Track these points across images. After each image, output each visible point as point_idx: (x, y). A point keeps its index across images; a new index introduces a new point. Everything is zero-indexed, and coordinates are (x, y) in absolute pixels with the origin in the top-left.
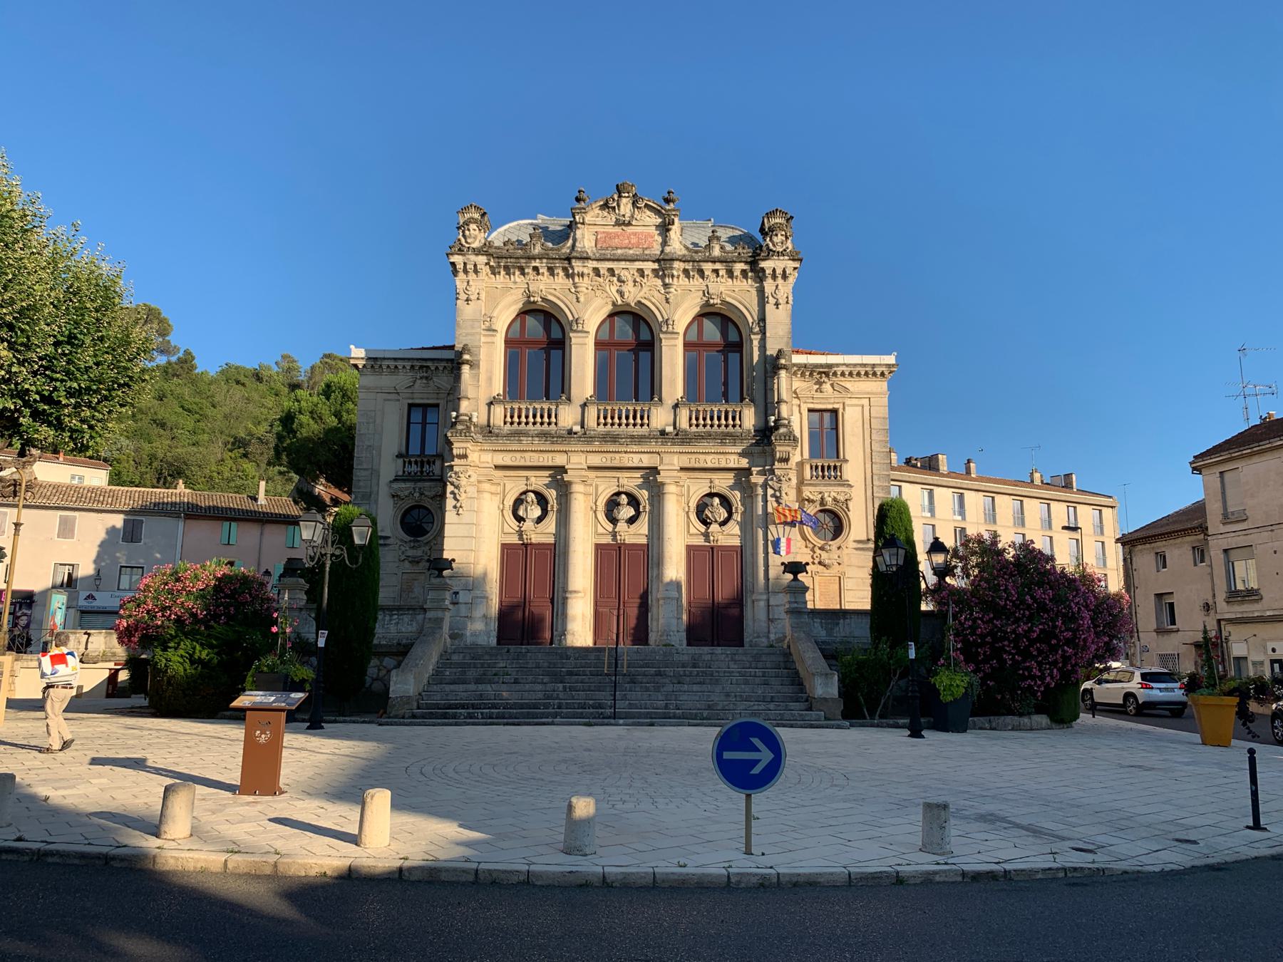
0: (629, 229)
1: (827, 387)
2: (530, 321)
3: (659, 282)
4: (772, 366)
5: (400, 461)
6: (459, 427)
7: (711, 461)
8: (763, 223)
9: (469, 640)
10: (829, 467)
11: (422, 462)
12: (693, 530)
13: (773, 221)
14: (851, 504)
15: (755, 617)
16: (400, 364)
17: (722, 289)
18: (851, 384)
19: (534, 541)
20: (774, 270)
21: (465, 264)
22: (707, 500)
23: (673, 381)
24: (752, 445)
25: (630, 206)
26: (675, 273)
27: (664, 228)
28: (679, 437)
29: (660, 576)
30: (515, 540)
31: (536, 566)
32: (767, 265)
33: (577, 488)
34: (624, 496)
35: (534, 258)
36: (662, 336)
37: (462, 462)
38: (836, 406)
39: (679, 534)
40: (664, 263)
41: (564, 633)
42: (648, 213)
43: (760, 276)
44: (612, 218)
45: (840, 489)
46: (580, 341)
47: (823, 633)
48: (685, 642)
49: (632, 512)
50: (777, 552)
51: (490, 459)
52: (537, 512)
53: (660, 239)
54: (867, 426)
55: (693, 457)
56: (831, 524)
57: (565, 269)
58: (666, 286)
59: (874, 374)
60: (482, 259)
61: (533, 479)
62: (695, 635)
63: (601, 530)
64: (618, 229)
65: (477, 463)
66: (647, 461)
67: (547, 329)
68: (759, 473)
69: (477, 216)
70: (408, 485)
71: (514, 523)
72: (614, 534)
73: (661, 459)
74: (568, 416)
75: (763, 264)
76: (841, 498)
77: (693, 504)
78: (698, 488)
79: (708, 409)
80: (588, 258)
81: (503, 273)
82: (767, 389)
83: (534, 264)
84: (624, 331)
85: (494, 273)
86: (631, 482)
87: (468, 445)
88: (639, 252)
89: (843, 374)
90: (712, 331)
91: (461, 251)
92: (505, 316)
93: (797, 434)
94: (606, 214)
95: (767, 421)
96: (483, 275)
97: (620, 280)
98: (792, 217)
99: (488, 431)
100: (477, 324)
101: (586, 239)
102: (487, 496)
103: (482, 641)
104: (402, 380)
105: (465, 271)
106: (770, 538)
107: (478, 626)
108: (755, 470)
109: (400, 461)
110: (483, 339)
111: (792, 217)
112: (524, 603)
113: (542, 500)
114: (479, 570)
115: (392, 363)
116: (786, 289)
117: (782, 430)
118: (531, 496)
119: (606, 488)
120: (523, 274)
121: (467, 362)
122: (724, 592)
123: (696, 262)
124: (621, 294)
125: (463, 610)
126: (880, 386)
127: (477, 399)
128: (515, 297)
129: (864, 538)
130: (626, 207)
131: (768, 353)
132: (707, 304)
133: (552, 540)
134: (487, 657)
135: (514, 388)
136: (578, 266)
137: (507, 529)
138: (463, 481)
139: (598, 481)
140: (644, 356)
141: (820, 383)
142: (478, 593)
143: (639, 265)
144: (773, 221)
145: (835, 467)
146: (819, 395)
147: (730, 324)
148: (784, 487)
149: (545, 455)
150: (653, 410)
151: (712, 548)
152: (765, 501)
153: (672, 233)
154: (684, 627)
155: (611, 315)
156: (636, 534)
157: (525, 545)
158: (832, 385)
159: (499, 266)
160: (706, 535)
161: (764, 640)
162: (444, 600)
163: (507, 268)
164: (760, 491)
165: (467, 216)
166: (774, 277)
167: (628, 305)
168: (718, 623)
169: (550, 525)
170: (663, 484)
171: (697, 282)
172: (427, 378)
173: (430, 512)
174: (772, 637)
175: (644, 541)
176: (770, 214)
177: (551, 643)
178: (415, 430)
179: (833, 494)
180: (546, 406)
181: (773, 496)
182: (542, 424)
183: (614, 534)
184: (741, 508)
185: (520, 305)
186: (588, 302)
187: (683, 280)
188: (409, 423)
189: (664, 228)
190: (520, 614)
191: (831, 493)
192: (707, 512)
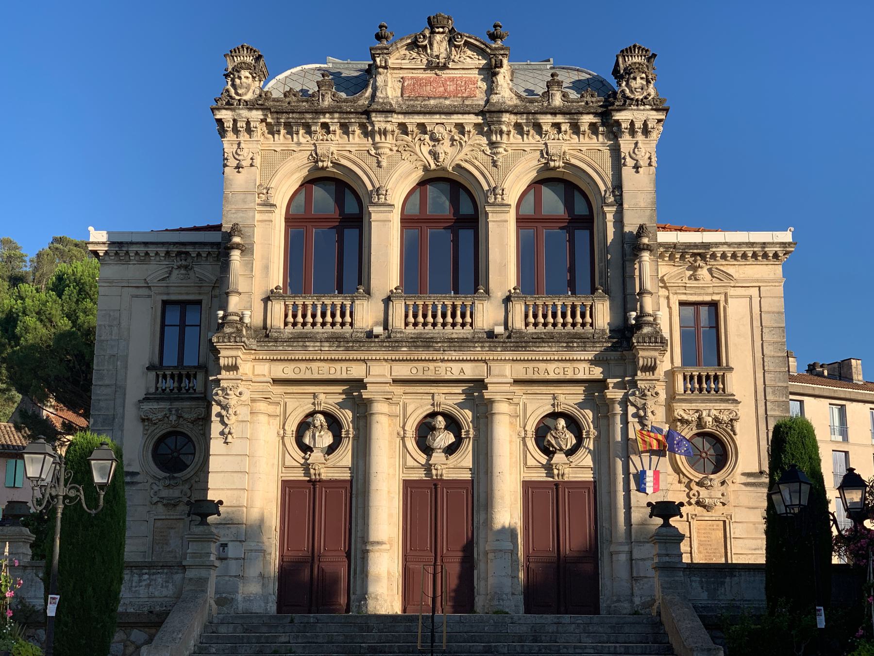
0: (445, 74)
1: (703, 273)
2: (318, 192)
3: (484, 140)
4: (632, 246)
5: (152, 375)
6: (228, 330)
7: (553, 371)
8: (617, 64)
9: (241, 606)
10: (708, 377)
11: (180, 376)
12: (531, 462)
13: (630, 60)
14: (737, 426)
15: (614, 575)
16: (152, 250)
17: (565, 148)
18: (737, 270)
19: (324, 477)
20: (632, 123)
21: (235, 121)
22: (549, 422)
23: (504, 266)
24: (607, 349)
25: (445, 44)
26: (504, 128)
27: (490, 72)
28: (512, 341)
29: (488, 520)
30: (299, 475)
31: (327, 509)
32: (623, 117)
33: (380, 407)
34: (440, 418)
35: (324, 113)
36: (488, 209)
37: (232, 375)
38: (716, 298)
39: (513, 467)
40: (489, 117)
41: (364, 596)
42: (469, 53)
43: (613, 131)
45: (723, 406)
46: (382, 216)
47: (705, 595)
48: (522, 608)
49: (451, 438)
50: (641, 489)
51: (266, 370)
52: (326, 439)
53: (484, 86)
54: (756, 323)
55: (531, 365)
56: (712, 452)
57: (363, 126)
58: (492, 144)
59: (765, 256)
60: (256, 115)
61: (322, 397)
62: (536, 597)
63: (410, 462)
64: (430, 74)
65: (251, 376)
66: (470, 371)
67: (340, 201)
68: (617, 386)
69: (249, 60)
71: (298, 454)
72: (428, 468)
73: (489, 370)
74: (367, 315)
76: (725, 417)
77: (531, 427)
78: (538, 406)
79: (550, 303)
80: (392, 112)
81: (283, 131)
83: (322, 120)
84: (440, 203)
85: (272, 133)
86: (449, 399)
87: (239, 353)
88: (457, 102)
89: (724, 256)
90: (552, 203)
91: (229, 106)
92: (286, 184)
93: (666, 334)
94: (415, 55)
95: (626, 319)
96: (257, 135)
97: (433, 138)
98: (654, 56)
99: (265, 334)
100: (249, 198)
101: (389, 87)
102: (263, 419)
103: (257, 607)
104: (154, 270)
105: (236, 131)
106: (632, 470)
107: (253, 588)
108: (611, 381)
109: (152, 375)
110: (258, 216)
111: (654, 56)
112: (312, 558)
113: (334, 424)
114: (254, 514)
115: (142, 249)
116: (647, 148)
117: (646, 330)
119: (417, 407)
120: (309, 132)
121: (237, 246)
122: (573, 541)
123: (531, 113)
124: (435, 155)
125: (233, 568)
126: (772, 272)
127: (250, 293)
128: (298, 163)
129: (756, 469)
130: (440, 46)
131: (627, 229)
132: (546, 168)
133: (347, 476)
134: (264, 629)
135: (297, 278)
136: (379, 122)
137: (289, 462)
138: (233, 400)
139: (407, 399)
140: (466, 235)
141: (694, 268)
142: (253, 545)
144: (630, 60)
145: (716, 377)
146: (694, 283)
147: (576, 193)
148: (650, 403)
149: (338, 366)
150: (478, 306)
151: (557, 484)
152: (625, 422)
153: (500, 78)
154: (520, 588)
155: (422, 184)
156: (458, 467)
157: (313, 482)
158: (710, 271)
159: (278, 124)
160: (549, 468)
161: (626, 605)
162: (208, 554)
163: (288, 126)
164: (618, 409)
165: (238, 60)
166: (632, 131)
167: (444, 169)
168: (566, 581)
169: (345, 456)
170: (491, 402)
171: (533, 139)
172: (186, 267)
173: (190, 439)
174: (637, 600)
175: (467, 476)
176: (626, 52)
177: (348, 610)
178: (172, 334)
179: (713, 412)
180: (338, 302)
181: (634, 416)
182: (333, 324)
183: (428, 468)
184: (593, 432)
185: (305, 172)
186: (392, 165)
187: (515, 138)
188: (163, 325)
189: (490, 72)
190: (307, 572)
191: (711, 411)
192: (549, 437)
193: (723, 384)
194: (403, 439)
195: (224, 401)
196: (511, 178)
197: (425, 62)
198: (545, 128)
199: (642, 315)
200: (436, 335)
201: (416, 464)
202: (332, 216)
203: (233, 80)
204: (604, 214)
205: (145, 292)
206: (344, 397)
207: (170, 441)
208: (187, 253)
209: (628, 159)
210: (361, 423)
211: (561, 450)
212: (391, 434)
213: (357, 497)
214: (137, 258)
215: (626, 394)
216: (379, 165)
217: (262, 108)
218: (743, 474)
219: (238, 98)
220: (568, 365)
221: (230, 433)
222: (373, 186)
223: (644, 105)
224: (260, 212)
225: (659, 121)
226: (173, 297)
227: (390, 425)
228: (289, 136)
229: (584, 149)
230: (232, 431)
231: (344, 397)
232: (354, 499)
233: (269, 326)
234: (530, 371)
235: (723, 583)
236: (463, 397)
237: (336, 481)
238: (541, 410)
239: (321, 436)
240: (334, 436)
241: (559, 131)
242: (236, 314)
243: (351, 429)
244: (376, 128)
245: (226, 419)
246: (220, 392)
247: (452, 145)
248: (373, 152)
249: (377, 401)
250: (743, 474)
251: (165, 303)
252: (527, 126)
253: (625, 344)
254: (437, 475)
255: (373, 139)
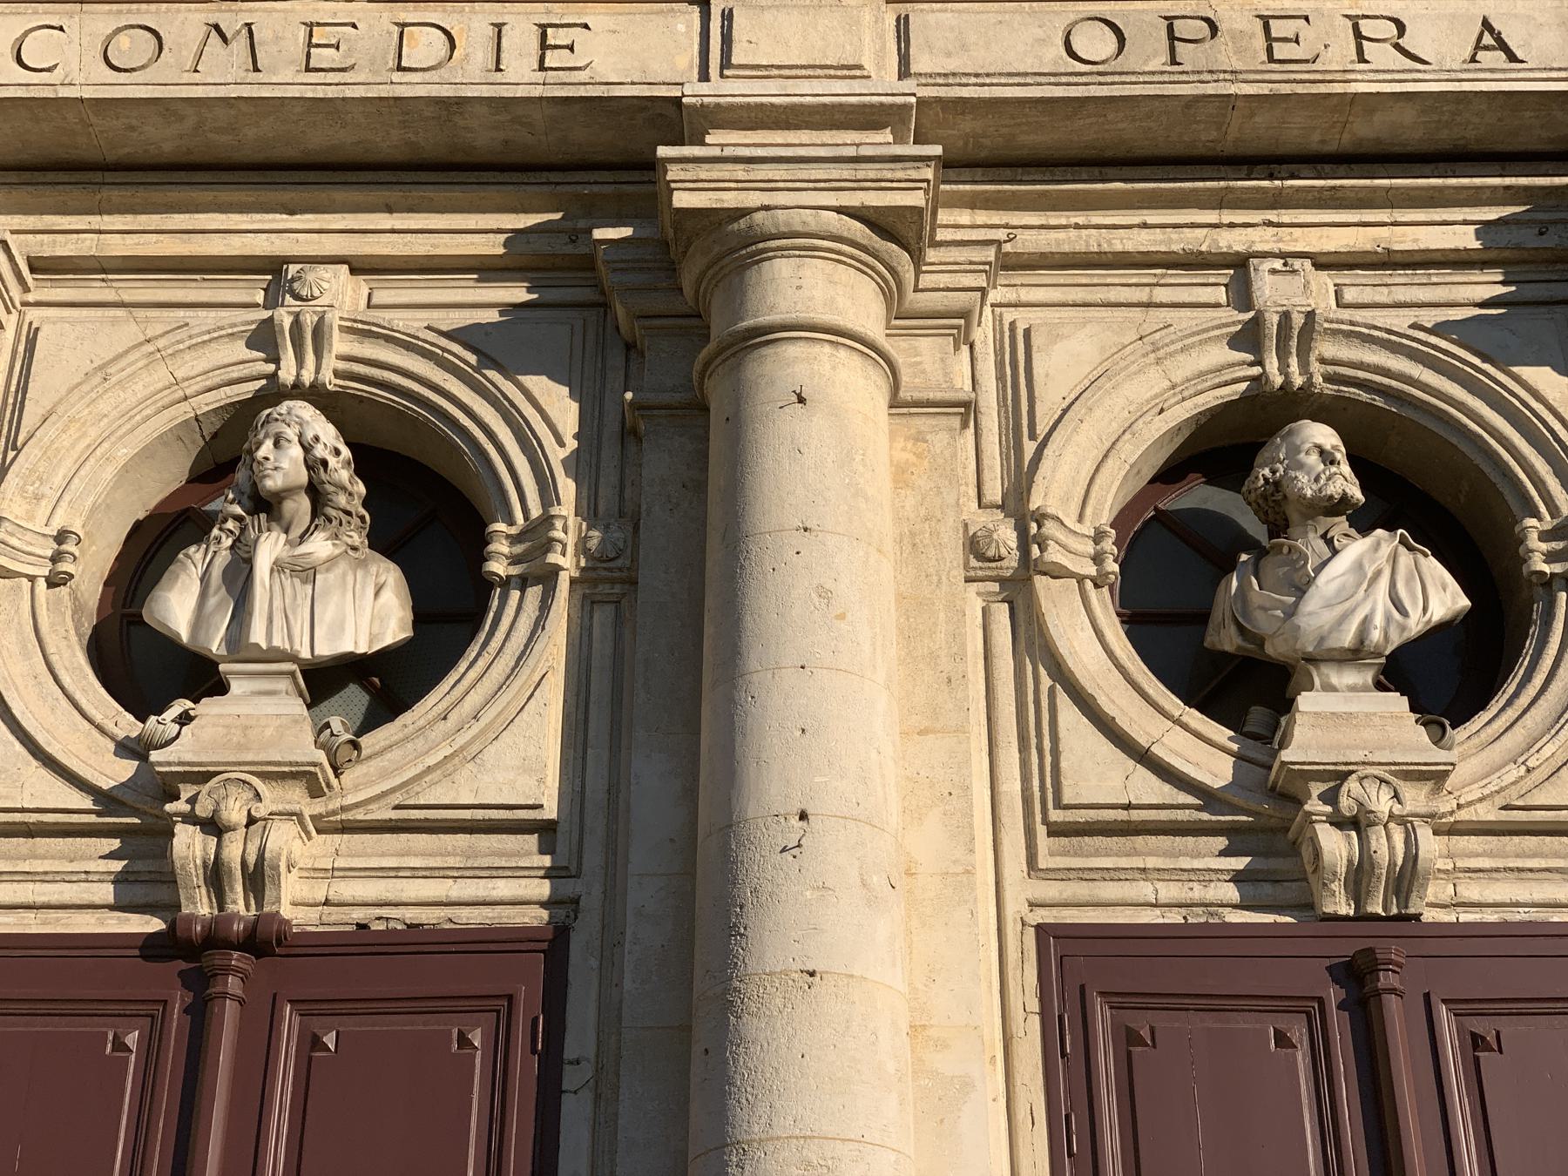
19: (296, 902)
63: (1096, 775)
71: (87, 730)
72: (1266, 822)
113: (423, 503)
157: (188, 953)
169: (507, 730)
194: (1017, 591)
201: (1148, 788)
206: (518, 293)
210: (659, 462)
212: (911, 543)
213: (604, 1091)
227: (901, 476)
231: (518, 293)
232: (575, 1113)
236: (1487, 285)
237: (417, 943)
239: (307, 573)
240: (422, 617)
249: (802, 242)
254: (1359, 876)
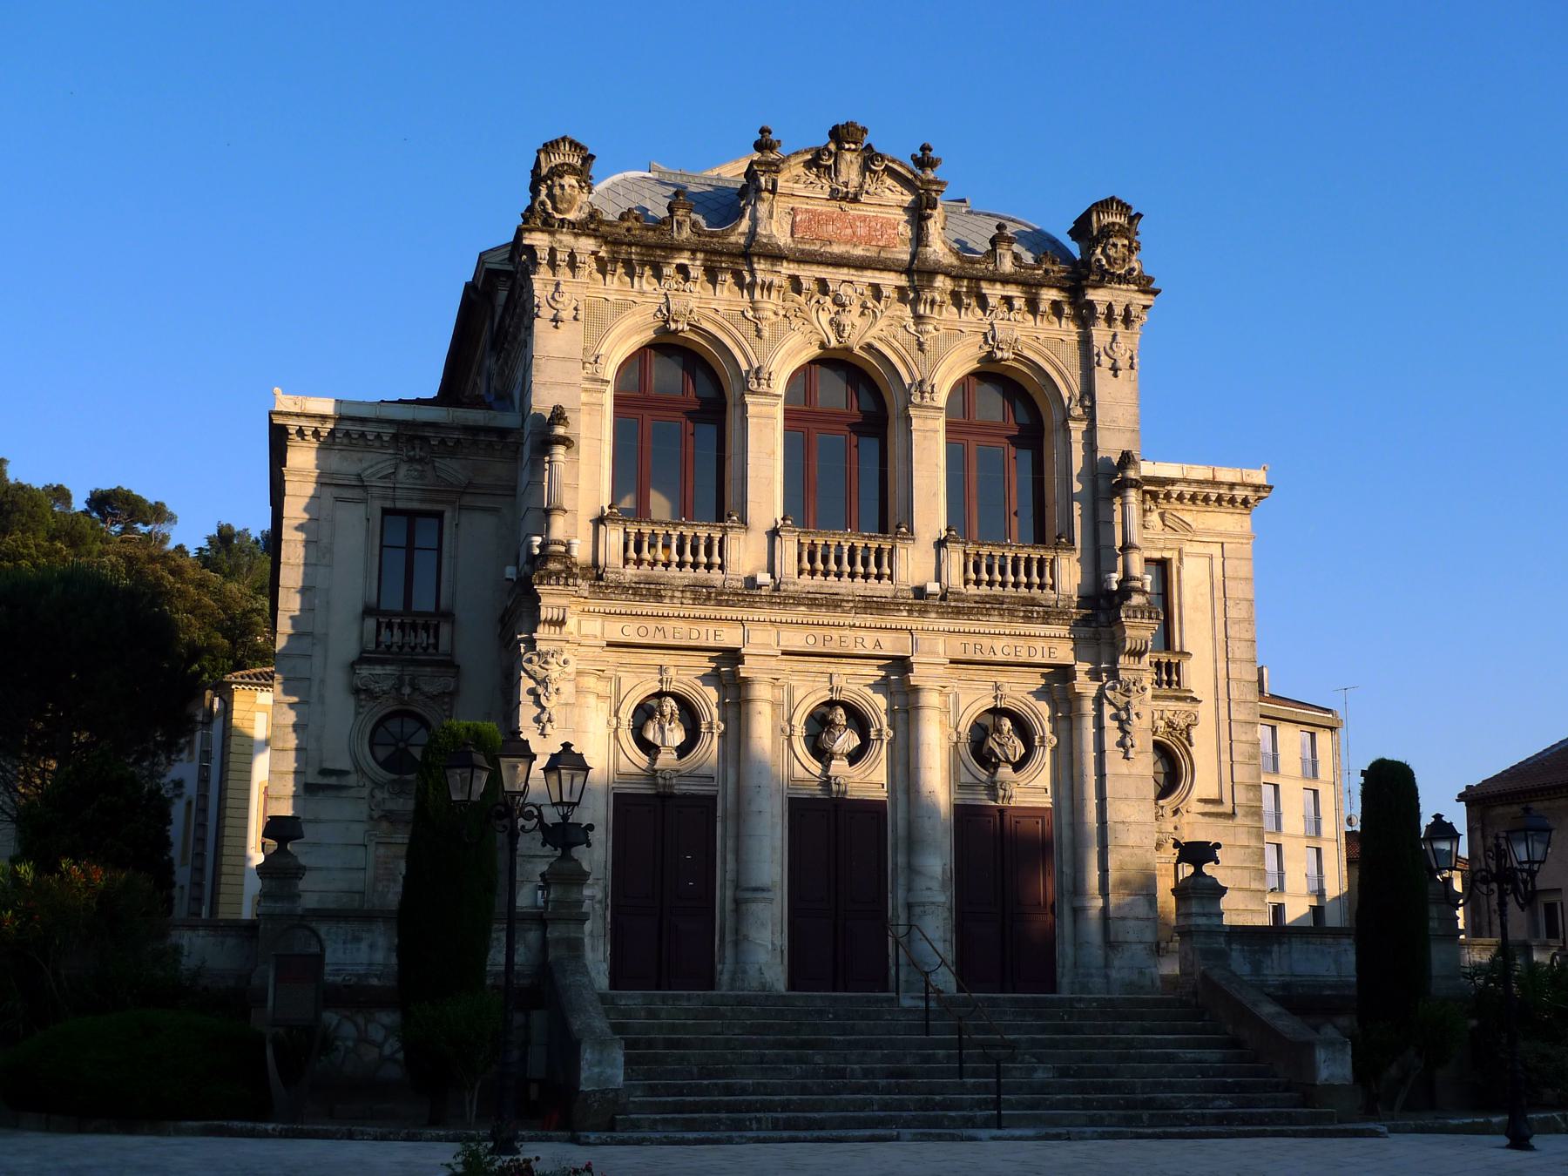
0: (853, 210)
5: (371, 623)
7: (1001, 649)
14: (1194, 732)
16: (369, 429)
18: (1193, 516)
21: (552, 251)
25: (856, 167)
28: (949, 604)
32: (1098, 296)
34: (841, 711)
36: (912, 412)
38: (1167, 555)
42: (889, 182)
44: (822, 188)
45: (1181, 705)
54: (1218, 594)
55: (972, 640)
57: (738, 277)
58: (919, 319)
60: (586, 245)
61: (672, 672)
66: (891, 645)
69: (576, 161)
70: (389, 669)
73: (915, 644)
75: (1093, 295)
76: (1181, 722)
78: (975, 699)
82: (1099, 525)
83: (678, 261)
88: (872, 253)
91: (548, 226)
94: (813, 178)
96: (583, 276)
101: (775, 223)
102: (592, 700)
105: (553, 264)
109: (371, 623)
111: (1139, 216)
118: (670, 705)
120: (658, 275)
123: (970, 281)
124: (838, 327)
127: (575, 513)
128: (638, 318)
129: (1214, 795)
130: (850, 169)
132: (989, 358)
138: (554, 671)
139: (795, 681)
143: (871, 277)
144: (1107, 219)
145: (1169, 664)
149: (703, 627)
150: (901, 551)
153: (930, 223)
158: (1162, 516)
159: (614, 261)
164: (1088, 707)
165: (556, 160)
166: (1110, 319)
167: (849, 350)
171: (973, 317)
179: (1168, 714)
180: (703, 533)
186: (777, 338)
189: (918, 214)
193: (1178, 675)
195: (541, 674)
196: (942, 369)
197: (826, 187)
198: (992, 301)
199: (1127, 577)
200: (842, 591)
202: (682, 399)
203: (550, 188)
204: (1068, 431)
205: (356, 493)
207: (410, 725)
208: (425, 440)
209: (1103, 357)
211: (1008, 761)
214: (345, 441)
215: (1102, 688)
216: (759, 336)
217: (594, 234)
218: (1200, 800)
219: (557, 216)
220: (1020, 642)
221: (549, 720)
222: (750, 365)
223: (1129, 283)
224: (586, 390)
225: (1145, 307)
226: (400, 505)
228: (628, 279)
229: (1042, 336)
230: (554, 717)
233: (601, 562)
234: (970, 648)
235: (1270, 953)
238: (978, 705)
241: (1011, 309)
242: (561, 543)
243: (716, 721)
244: (759, 281)
245: (543, 700)
246: (535, 658)
247: (863, 314)
248: (750, 314)
249: (760, 682)
250: (1200, 800)
251: (386, 512)
252: (968, 297)
253: (1102, 618)
255: (752, 295)
